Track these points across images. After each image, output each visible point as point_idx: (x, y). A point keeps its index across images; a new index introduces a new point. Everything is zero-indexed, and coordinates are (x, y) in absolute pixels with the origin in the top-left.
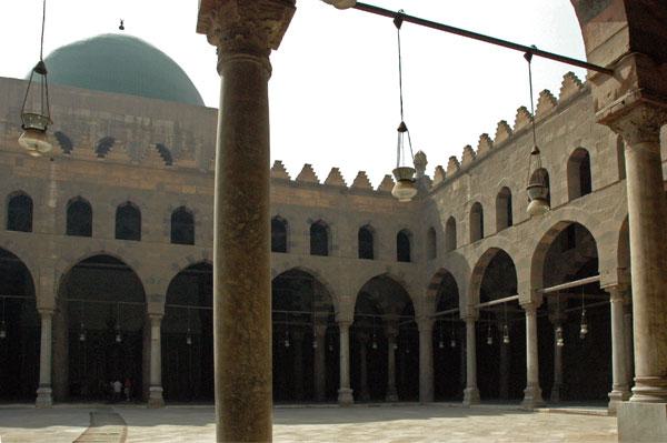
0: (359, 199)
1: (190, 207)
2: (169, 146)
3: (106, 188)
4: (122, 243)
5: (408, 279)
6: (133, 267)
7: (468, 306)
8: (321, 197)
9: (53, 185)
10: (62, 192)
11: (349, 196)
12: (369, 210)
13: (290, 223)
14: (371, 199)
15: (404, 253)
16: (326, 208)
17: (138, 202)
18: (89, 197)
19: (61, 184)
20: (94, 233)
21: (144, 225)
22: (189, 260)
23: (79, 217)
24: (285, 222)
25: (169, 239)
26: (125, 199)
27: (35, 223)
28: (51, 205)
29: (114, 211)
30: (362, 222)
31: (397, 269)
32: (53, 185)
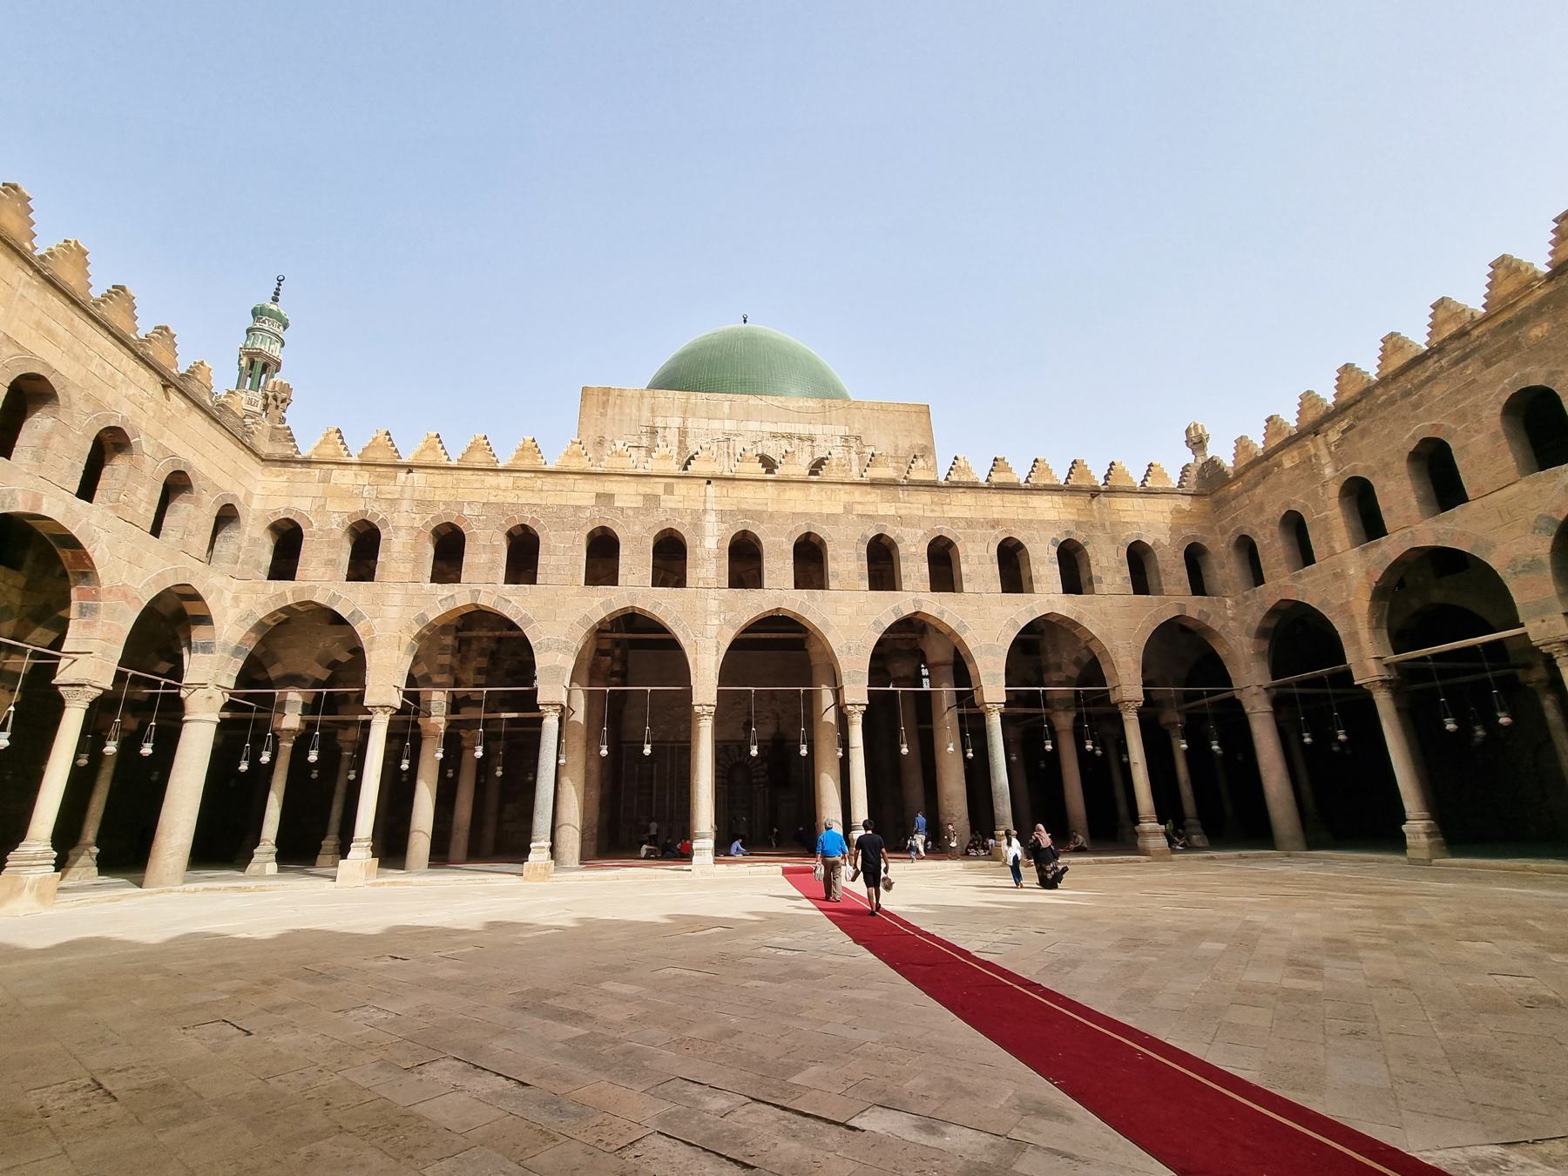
1: (892, 532)
5: (1215, 624)
7: (1367, 656)
9: (711, 518)
10: (723, 526)
11: (1103, 499)
15: (1198, 585)
17: (823, 531)
18: (759, 531)
20: (766, 583)
21: (832, 566)
23: (745, 561)
25: (866, 583)
30: (1130, 536)
31: (1194, 607)
32: (711, 518)
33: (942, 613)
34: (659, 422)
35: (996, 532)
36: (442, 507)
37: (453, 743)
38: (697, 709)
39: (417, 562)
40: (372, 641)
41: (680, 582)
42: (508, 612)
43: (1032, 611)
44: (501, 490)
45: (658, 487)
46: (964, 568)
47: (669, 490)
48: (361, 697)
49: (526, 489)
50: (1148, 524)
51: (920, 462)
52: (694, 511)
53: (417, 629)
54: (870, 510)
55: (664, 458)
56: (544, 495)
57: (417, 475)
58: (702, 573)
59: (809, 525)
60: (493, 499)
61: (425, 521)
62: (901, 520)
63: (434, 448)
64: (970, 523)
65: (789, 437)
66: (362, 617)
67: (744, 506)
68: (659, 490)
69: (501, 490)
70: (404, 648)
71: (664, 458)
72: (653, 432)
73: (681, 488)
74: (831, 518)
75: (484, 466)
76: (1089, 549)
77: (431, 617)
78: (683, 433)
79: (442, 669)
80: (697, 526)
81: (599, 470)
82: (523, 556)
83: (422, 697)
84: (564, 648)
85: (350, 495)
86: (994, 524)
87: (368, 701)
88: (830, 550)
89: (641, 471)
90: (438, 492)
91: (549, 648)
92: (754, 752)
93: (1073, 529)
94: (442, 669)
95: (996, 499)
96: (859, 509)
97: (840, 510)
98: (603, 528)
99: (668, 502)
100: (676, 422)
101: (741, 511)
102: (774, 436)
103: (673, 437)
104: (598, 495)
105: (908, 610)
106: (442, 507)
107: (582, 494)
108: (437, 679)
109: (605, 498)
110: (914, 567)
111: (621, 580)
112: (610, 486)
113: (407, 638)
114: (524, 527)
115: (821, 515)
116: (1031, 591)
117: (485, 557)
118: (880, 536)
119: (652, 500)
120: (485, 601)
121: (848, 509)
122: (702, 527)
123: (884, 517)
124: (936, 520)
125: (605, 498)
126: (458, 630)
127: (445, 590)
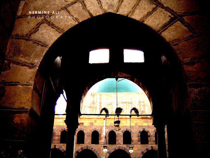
2: (137, 108)
4: (125, 146)
23: (112, 137)
25: (140, 143)
27: (100, 141)
28: (104, 133)
29: (122, 134)
32: (104, 128)
47: (95, 121)
54: (141, 124)
59: (127, 129)
60: (59, 125)
68: (93, 121)
80: (101, 130)
88: (132, 134)
96: (139, 124)
105: (150, 149)
111: (85, 143)
119: (92, 124)
121: (136, 124)
123: (145, 126)
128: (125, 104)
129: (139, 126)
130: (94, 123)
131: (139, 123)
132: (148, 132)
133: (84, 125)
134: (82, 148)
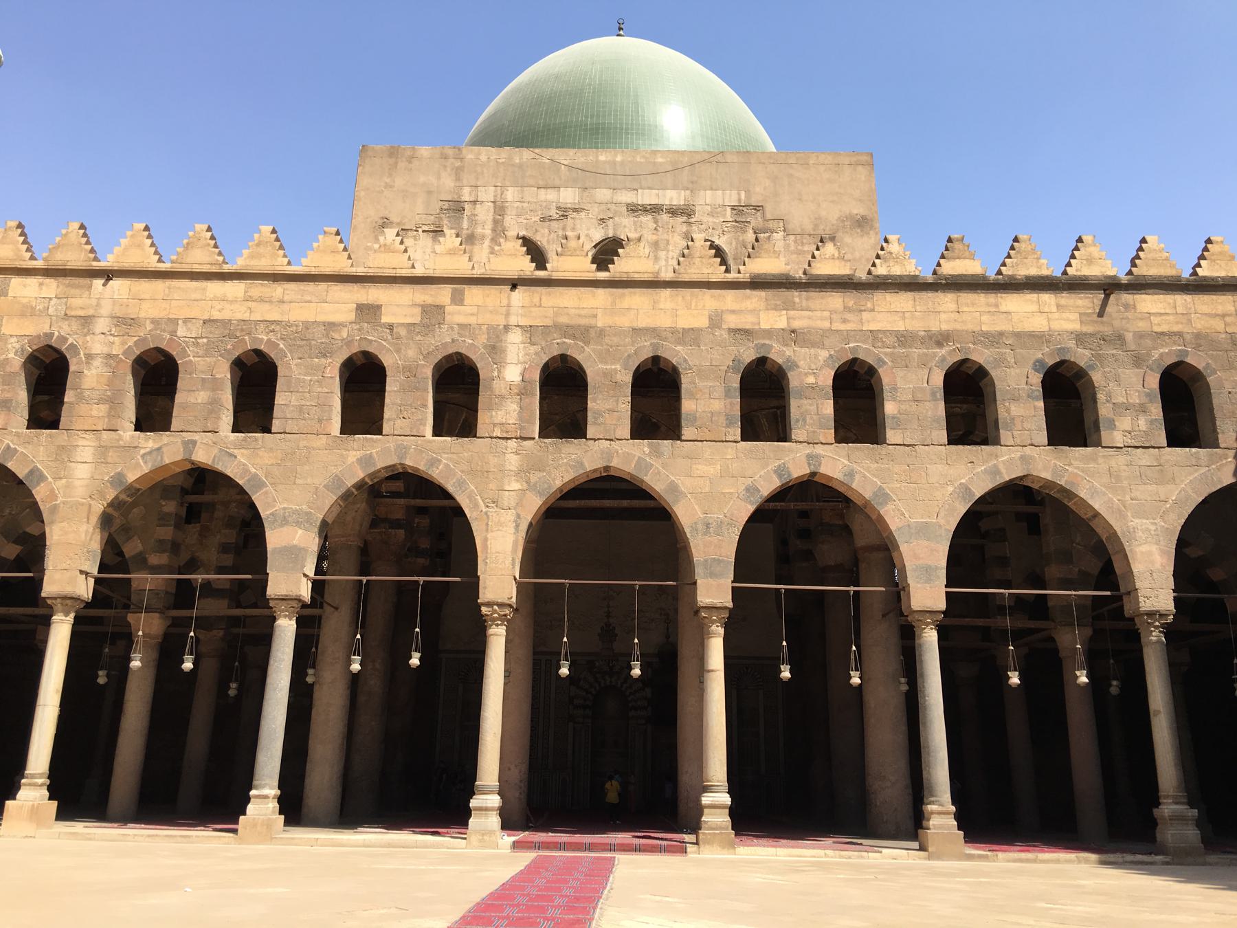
0: (1149, 303)
1: (779, 353)
3: (615, 330)
4: (644, 446)
6: (668, 499)
8: (1058, 306)
9: (515, 339)
10: (533, 349)
12: (1176, 328)
13: (993, 373)
14: (1182, 301)
16: (1080, 338)
17: (676, 354)
19: (529, 330)
20: (590, 432)
21: (687, 405)
22: (780, 476)
23: (562, 395)
24: (982, 372)
25: (737, 432)
26: (647, 354)
27: (485, 419)
28: (511, 376)
32: (515, 339)
33: (851, 474)
34: (466, 195)
35: (943, 351)
36: (149, 327)
37: (168, 652)
38: (484, 610)
39: (113, 402)
40: (54, 509)
41: (467, 428)
42: (230, 470)
43: (995, 472)
44: (228, 301)
45: (443, 294)
46: (890, 408)
47: (458, 299)
48: (37, 583)
49: (262, 300)
50: (1198, 336)
51: (829, 248)
52: (492, 329)
53: (111, 495)
54: (746, 322)
55: (451, 252)
56: (286, 307)
57: (115, 283)
58: (499, 416)
60: (216, 315)
61: (124, 347)
62: (794, 335)
63: (140, 246)
64: (904, 339)
65: (655, 210)
66: (42, 478)
67: (563, 320)
69: (228, 301)
70: (95, 519)
71: (451, 252)
72: (456, 208)
73: (474, 295)
74: (690, 336)
75: (206, 268)
76: (1096, 377)
77: (131, 477)
78: (500, 209)
79: (161, 546)
80: (495, 350)
81: (360, 271)
82: (255, 388)
83: (134, 585)
84: (300, 520)
85: (27, 312)
86: (941, 339)
87: (50, 588)
89: (419, 271)
90: (145, 306)
91: (285, 521)
92: (636, 672)
93: (1071, 344)
94: (161, 546)
95: (947, 301)
96: (732, 321)
97: (703, 322)
98: (366, 354)
99: (457, 315)
100: (487, 194)
101: (557, 326)
102: (634, 209)
103: (485, 213)
104: (361, 308)
105: (799, 470)
106: (149, 327)
107: (338, 305)
108: (154, 560)
109: (368, 312)
110: (812, 408)
111: (386, 428)
112: (374, 294)
113: (99, 507)
114: (258, 352)
115: (674, 331)
116: (996, 442)
117: (205, 392)
118: (762, 361)
119: (433, 313)
120: (202, 456)
121: (716, 321)
122: (504, 351)
123: (769, 333)
124: (847, 336)
125: (368, 312)
126: (184, 492)
127: (149, 441)
128: (646, 219)
129: (735, 331)
130: (449, 309)
131: (733, 312)
132: (791, 368)
133: (385, 319)
134: (365, 461)
